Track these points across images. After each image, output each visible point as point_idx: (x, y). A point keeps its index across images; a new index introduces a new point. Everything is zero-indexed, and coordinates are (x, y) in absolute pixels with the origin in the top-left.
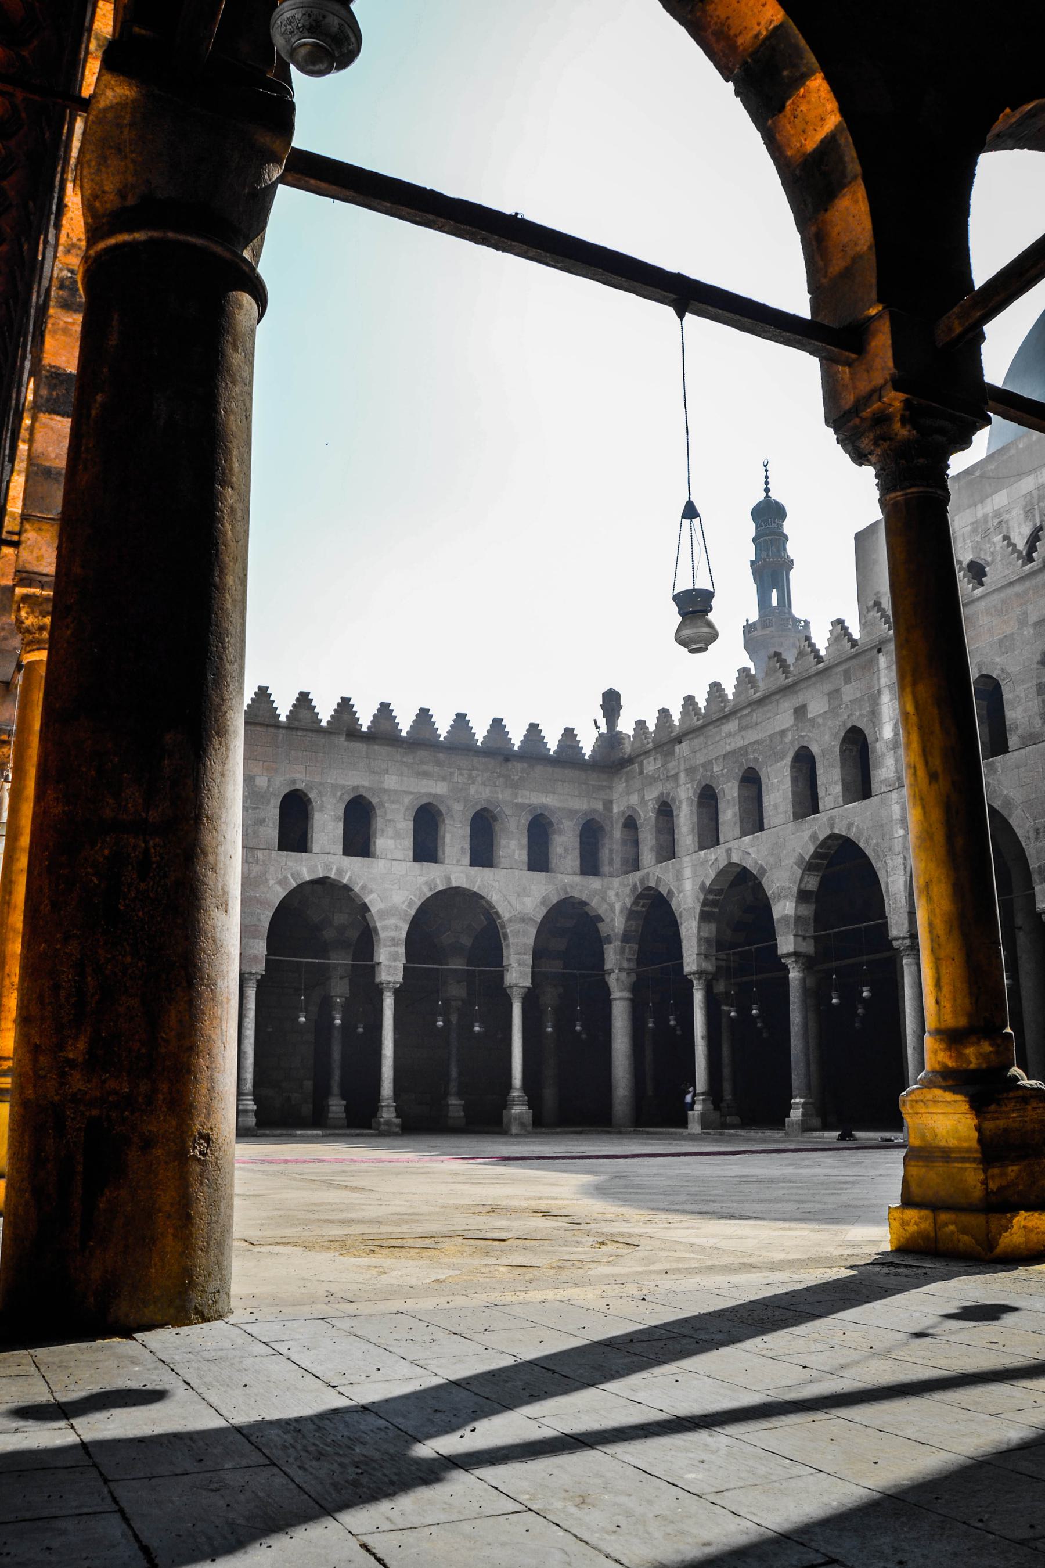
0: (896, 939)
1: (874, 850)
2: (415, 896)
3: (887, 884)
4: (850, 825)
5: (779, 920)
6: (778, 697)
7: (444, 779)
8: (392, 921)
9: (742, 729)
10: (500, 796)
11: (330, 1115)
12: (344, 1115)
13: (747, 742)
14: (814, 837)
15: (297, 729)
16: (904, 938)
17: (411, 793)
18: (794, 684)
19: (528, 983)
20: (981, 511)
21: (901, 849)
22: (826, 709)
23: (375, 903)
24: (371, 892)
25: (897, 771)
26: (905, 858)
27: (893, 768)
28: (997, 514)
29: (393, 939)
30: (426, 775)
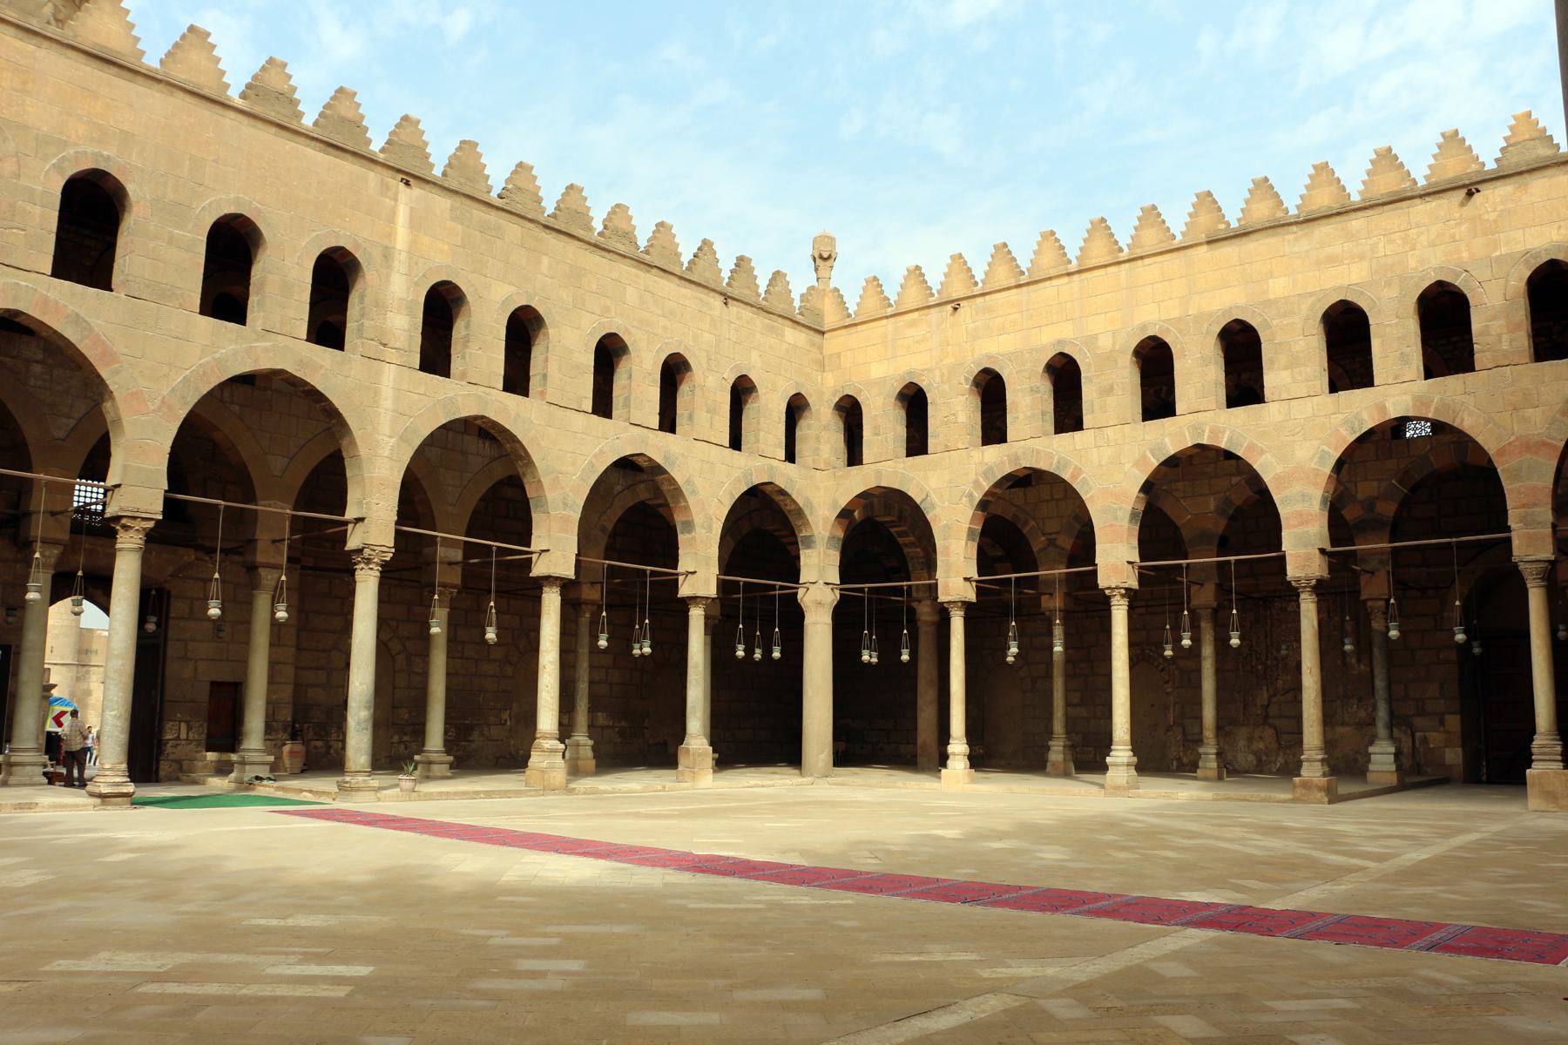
2: (1329, 445)
7: (1362, 257)
8: (1297, 488)
10: (1465, 255)
11: (1371, 767)
12: (1393, 768)
15: (1141, 258)
17: (1311, 294)
19: (1547, 553)
23: (1268, 468)
24: (1262, 452)
29: (1300, 515)
30: (1332, 260)
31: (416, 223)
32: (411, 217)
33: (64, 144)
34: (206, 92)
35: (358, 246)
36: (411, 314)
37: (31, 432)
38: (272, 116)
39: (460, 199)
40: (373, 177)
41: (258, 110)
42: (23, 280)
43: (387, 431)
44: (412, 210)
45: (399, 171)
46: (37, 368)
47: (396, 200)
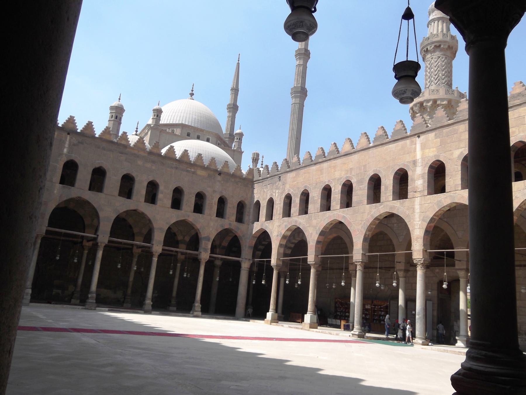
31: (424, 147)
32: (421, 146)
33: (341, 178)
34: (365, 147)
35: (405, 165)
36: (423, 177)
37: (395, 242)
38: (379, 143)
39: (437, 132)
40: (408, 141)
41: (376, 144)
42: (335, 212)
43: (418, 220)
44: (421, 144)
45: (415, 135)
46: (395, 225)
47: (416, 144)
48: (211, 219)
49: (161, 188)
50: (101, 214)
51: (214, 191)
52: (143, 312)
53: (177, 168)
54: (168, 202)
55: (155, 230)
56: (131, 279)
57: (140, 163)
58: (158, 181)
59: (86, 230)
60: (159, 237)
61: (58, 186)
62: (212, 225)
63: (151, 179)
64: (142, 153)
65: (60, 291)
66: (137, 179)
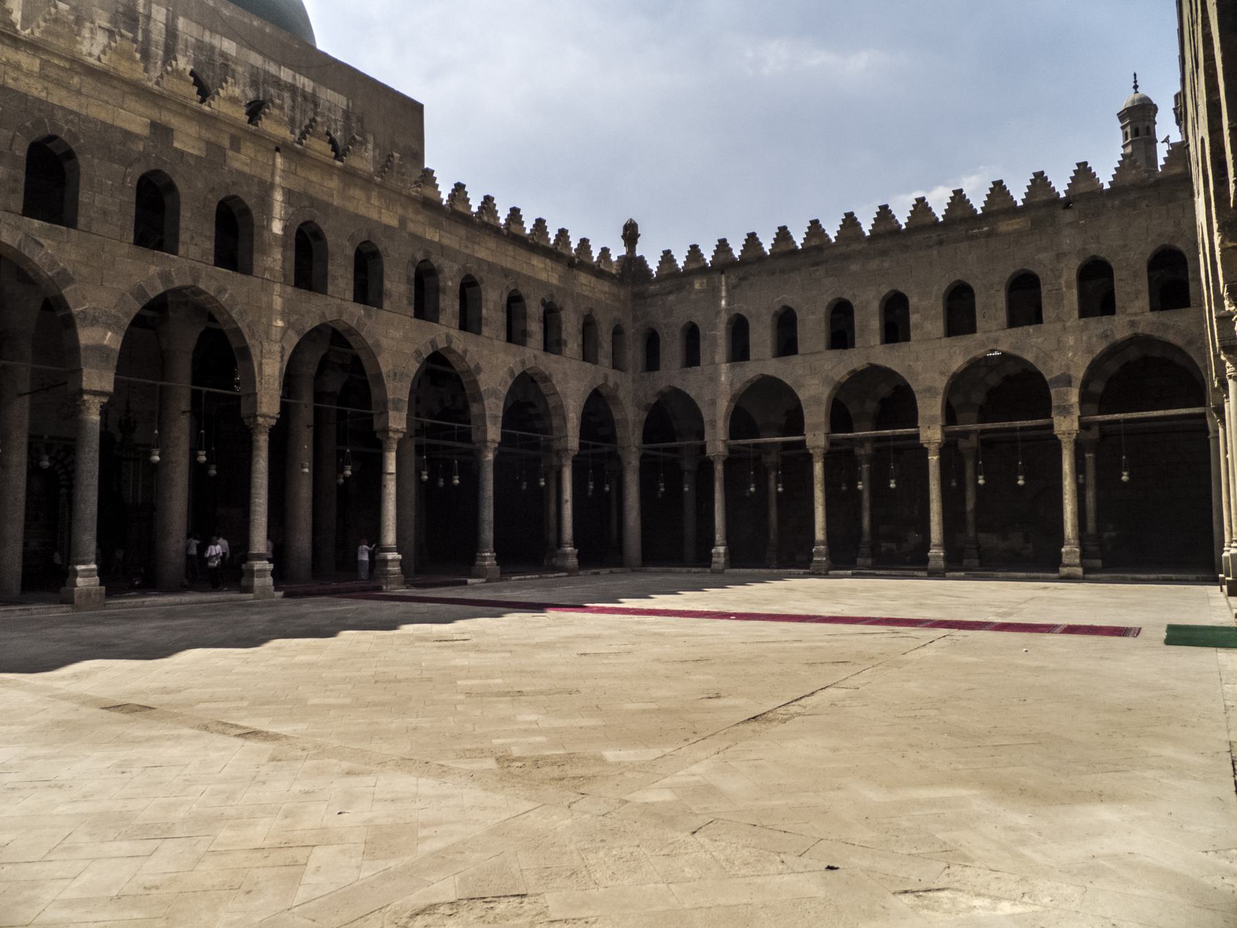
0: (263, 416)
1: (249, 326)
3: (261, 364)
4: (222, 290)
5: (87, 347)
6: (126, 89)
9: (43, 76)
13: (54, 100)
14: (165, 277)
16: (272, 418)
18: (161, 96)
20: (207, 37)
21: (278, 337)
22: (203, 154)
25: (283, 268)
26: (283, 348)
27: (280, 263)
28: (223, 55)
48: (1064, 329)
49: (913, 301)
50: (802, 395)
51: (1060, 256)
52: (924, 574)
53: (941, 243)
54: (938, 327)
55: (917, 396)
56: (970, 505)
57: (854, 267)
58: (901, 289)
59: (855, 426)
60: (930, 409)
61: (724, 367)
62: (1071, 343)
63: (885, 290)
64: (856, 246)
65: (894, 546)
66: (855, 304)
